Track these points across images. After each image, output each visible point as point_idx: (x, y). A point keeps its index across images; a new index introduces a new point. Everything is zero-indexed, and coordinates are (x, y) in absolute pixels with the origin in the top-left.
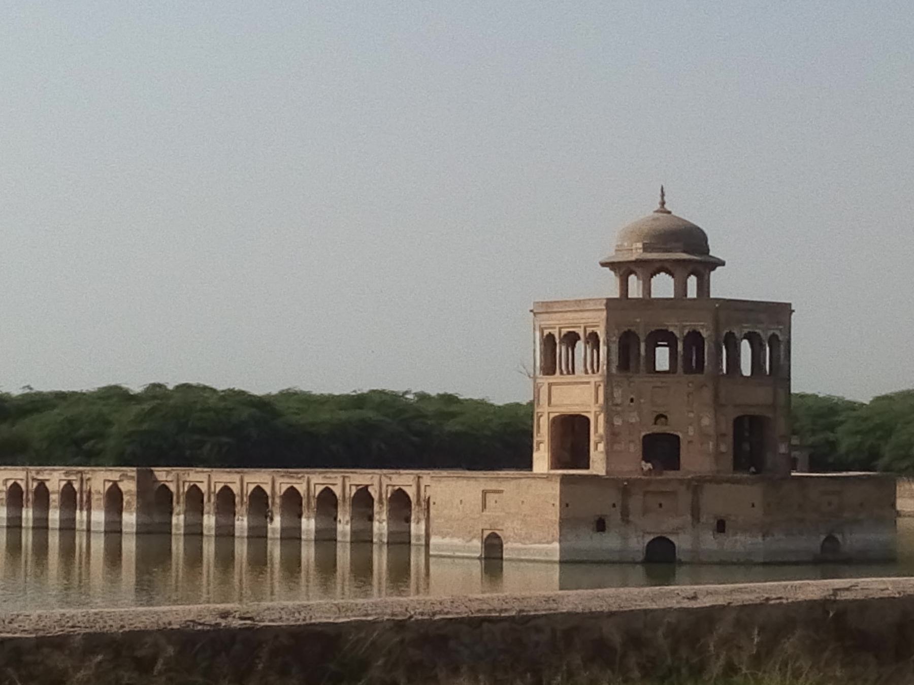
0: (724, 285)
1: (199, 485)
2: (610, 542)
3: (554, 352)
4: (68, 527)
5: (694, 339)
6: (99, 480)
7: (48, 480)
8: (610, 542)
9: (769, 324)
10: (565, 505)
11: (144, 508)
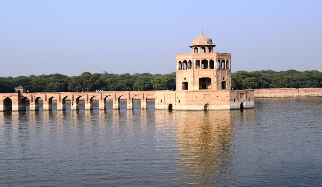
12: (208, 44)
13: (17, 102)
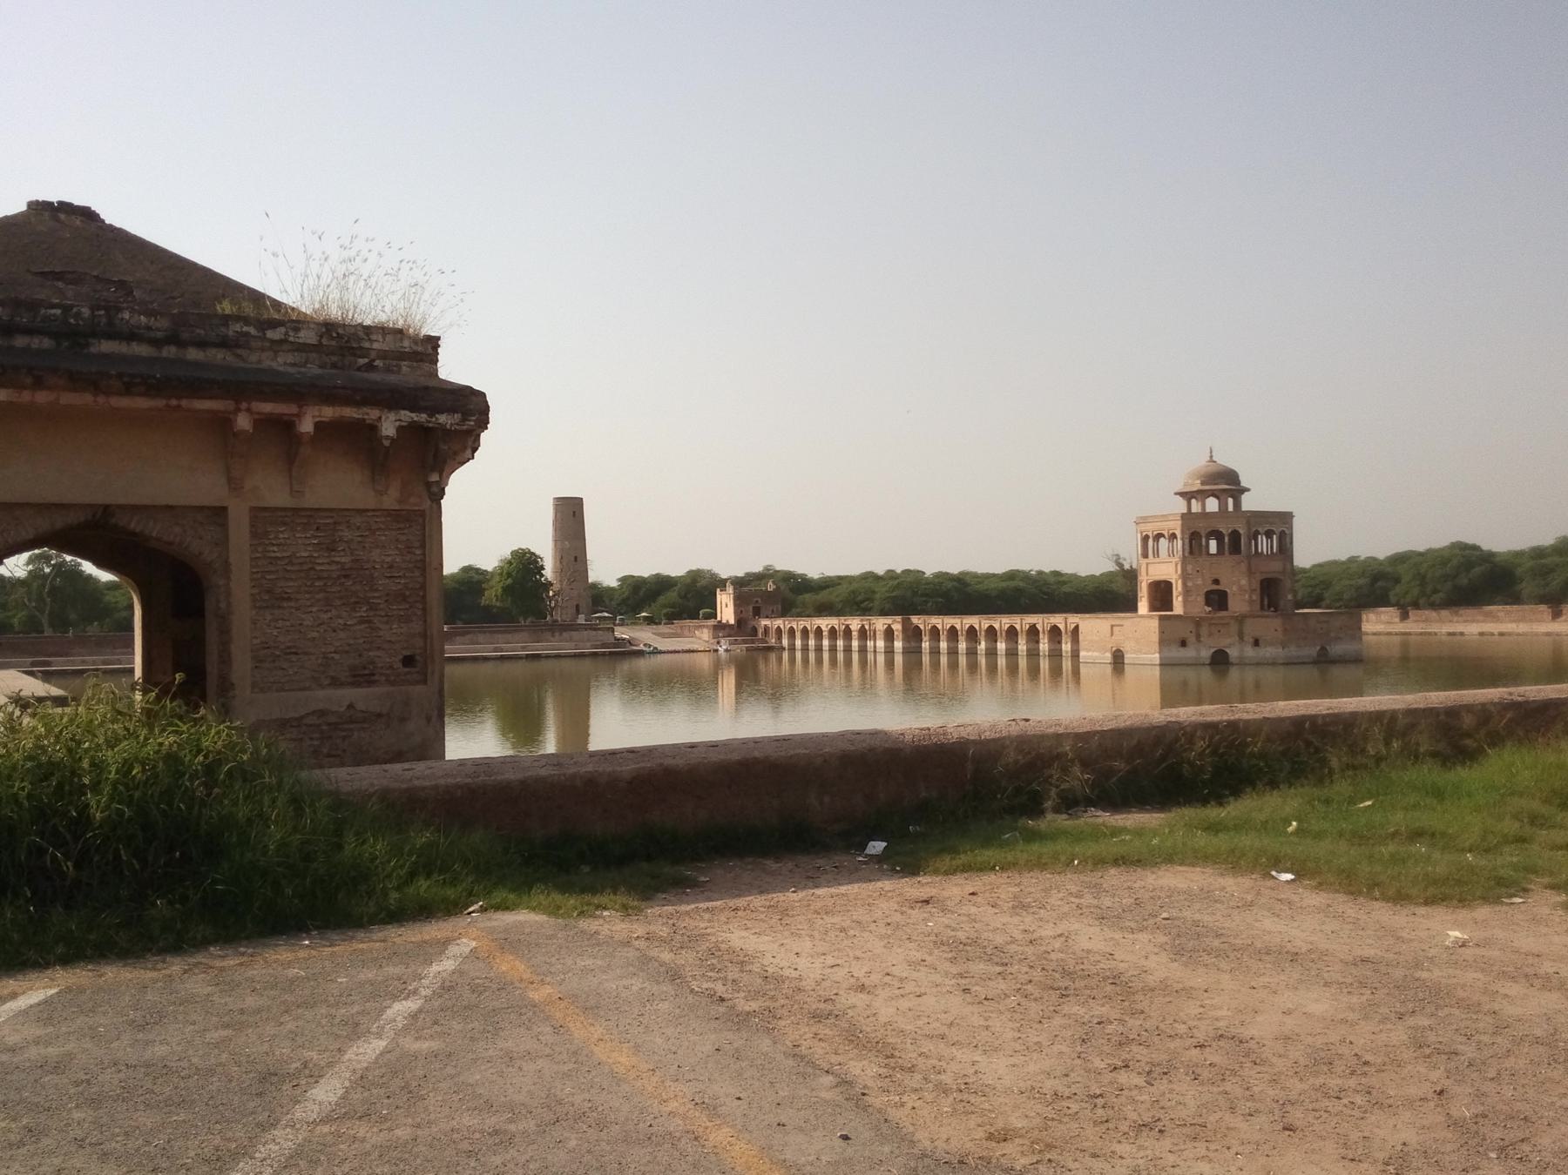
0: (1249, 503)
2: (1189, 653)
3: (1148, 543)
4: (863, 650)
5: (1235, 535)
8: (1189, 653)
9: (1278, 525)
10: (1162, 632)
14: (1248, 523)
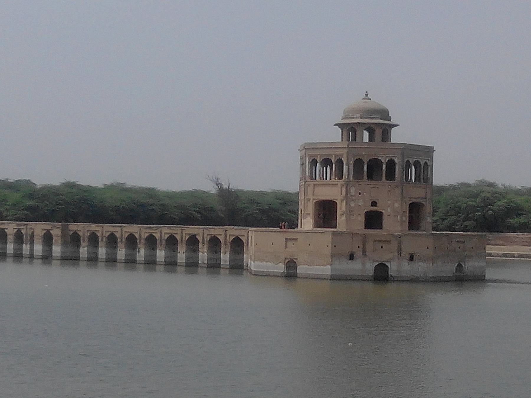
1: (97, 233)
5: (391, 164)
6: (39, 228)
7: (7, 229)
11: (64, 244)
12: (356, 121)
13: (60, 241)
14: (403, 155)
